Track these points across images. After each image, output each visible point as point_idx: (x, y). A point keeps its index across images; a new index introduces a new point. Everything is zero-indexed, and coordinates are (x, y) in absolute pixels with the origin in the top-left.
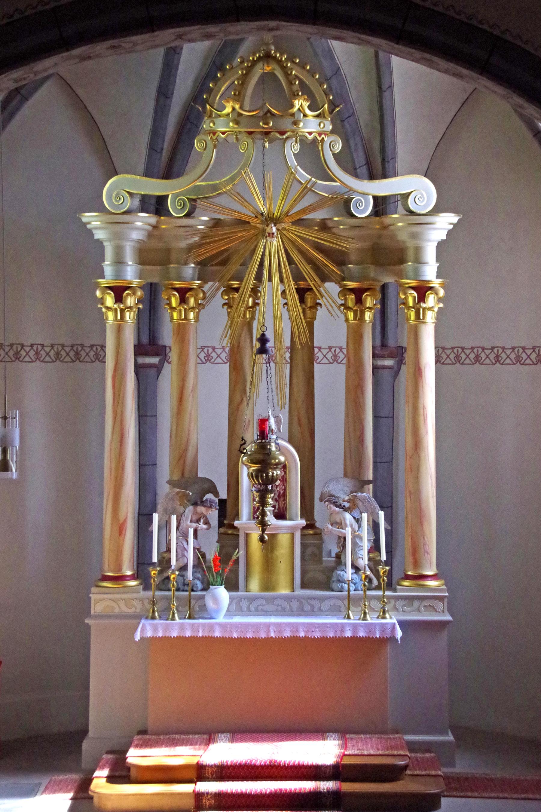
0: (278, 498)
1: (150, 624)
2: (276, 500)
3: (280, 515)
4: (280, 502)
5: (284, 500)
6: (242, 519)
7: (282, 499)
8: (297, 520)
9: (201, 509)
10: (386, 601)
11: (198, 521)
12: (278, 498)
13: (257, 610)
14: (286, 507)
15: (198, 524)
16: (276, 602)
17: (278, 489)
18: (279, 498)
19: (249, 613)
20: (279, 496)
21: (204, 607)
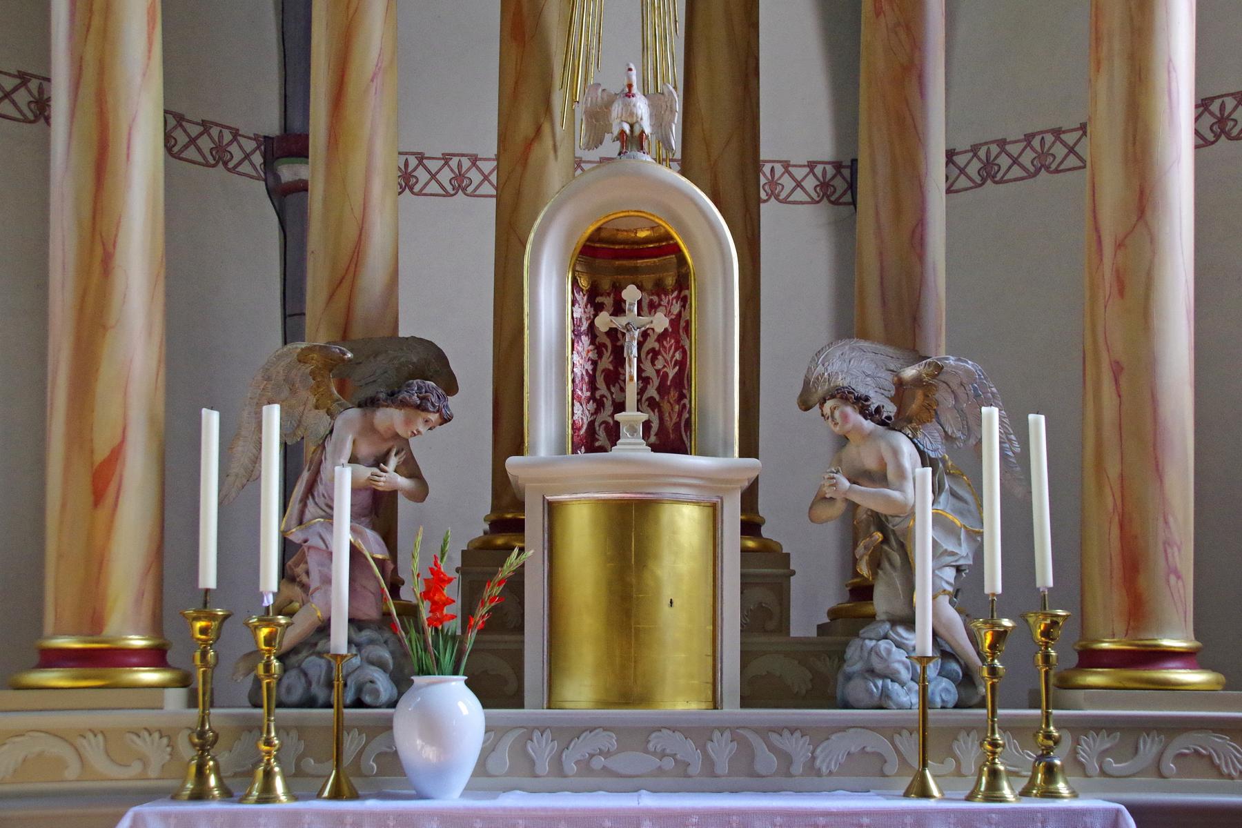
0: (657, 398)
1: (165, 816)
2: (653, 404)
3: (671, 437)
4: (666, 407)
5: (682, 396)
6: (534, 452)
7: (674, 394)
8: (727, 452)
9: (390, 418)
10: (1056, 734)
11: (380, 461)
12: (657, 398)
13: (585, 767)
14: (688, 423)
15: (376, 470)
16: (655, 742)
17: (659, 364)
18: (662, 397)
19: (558, 778)
20: (662, 389)
21: (392, 763)
